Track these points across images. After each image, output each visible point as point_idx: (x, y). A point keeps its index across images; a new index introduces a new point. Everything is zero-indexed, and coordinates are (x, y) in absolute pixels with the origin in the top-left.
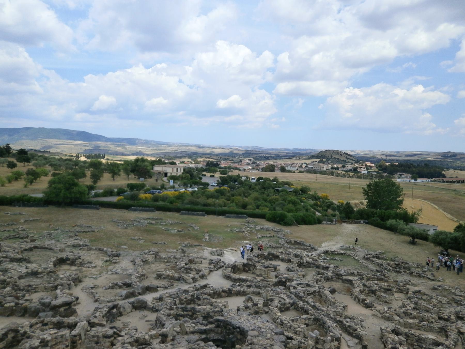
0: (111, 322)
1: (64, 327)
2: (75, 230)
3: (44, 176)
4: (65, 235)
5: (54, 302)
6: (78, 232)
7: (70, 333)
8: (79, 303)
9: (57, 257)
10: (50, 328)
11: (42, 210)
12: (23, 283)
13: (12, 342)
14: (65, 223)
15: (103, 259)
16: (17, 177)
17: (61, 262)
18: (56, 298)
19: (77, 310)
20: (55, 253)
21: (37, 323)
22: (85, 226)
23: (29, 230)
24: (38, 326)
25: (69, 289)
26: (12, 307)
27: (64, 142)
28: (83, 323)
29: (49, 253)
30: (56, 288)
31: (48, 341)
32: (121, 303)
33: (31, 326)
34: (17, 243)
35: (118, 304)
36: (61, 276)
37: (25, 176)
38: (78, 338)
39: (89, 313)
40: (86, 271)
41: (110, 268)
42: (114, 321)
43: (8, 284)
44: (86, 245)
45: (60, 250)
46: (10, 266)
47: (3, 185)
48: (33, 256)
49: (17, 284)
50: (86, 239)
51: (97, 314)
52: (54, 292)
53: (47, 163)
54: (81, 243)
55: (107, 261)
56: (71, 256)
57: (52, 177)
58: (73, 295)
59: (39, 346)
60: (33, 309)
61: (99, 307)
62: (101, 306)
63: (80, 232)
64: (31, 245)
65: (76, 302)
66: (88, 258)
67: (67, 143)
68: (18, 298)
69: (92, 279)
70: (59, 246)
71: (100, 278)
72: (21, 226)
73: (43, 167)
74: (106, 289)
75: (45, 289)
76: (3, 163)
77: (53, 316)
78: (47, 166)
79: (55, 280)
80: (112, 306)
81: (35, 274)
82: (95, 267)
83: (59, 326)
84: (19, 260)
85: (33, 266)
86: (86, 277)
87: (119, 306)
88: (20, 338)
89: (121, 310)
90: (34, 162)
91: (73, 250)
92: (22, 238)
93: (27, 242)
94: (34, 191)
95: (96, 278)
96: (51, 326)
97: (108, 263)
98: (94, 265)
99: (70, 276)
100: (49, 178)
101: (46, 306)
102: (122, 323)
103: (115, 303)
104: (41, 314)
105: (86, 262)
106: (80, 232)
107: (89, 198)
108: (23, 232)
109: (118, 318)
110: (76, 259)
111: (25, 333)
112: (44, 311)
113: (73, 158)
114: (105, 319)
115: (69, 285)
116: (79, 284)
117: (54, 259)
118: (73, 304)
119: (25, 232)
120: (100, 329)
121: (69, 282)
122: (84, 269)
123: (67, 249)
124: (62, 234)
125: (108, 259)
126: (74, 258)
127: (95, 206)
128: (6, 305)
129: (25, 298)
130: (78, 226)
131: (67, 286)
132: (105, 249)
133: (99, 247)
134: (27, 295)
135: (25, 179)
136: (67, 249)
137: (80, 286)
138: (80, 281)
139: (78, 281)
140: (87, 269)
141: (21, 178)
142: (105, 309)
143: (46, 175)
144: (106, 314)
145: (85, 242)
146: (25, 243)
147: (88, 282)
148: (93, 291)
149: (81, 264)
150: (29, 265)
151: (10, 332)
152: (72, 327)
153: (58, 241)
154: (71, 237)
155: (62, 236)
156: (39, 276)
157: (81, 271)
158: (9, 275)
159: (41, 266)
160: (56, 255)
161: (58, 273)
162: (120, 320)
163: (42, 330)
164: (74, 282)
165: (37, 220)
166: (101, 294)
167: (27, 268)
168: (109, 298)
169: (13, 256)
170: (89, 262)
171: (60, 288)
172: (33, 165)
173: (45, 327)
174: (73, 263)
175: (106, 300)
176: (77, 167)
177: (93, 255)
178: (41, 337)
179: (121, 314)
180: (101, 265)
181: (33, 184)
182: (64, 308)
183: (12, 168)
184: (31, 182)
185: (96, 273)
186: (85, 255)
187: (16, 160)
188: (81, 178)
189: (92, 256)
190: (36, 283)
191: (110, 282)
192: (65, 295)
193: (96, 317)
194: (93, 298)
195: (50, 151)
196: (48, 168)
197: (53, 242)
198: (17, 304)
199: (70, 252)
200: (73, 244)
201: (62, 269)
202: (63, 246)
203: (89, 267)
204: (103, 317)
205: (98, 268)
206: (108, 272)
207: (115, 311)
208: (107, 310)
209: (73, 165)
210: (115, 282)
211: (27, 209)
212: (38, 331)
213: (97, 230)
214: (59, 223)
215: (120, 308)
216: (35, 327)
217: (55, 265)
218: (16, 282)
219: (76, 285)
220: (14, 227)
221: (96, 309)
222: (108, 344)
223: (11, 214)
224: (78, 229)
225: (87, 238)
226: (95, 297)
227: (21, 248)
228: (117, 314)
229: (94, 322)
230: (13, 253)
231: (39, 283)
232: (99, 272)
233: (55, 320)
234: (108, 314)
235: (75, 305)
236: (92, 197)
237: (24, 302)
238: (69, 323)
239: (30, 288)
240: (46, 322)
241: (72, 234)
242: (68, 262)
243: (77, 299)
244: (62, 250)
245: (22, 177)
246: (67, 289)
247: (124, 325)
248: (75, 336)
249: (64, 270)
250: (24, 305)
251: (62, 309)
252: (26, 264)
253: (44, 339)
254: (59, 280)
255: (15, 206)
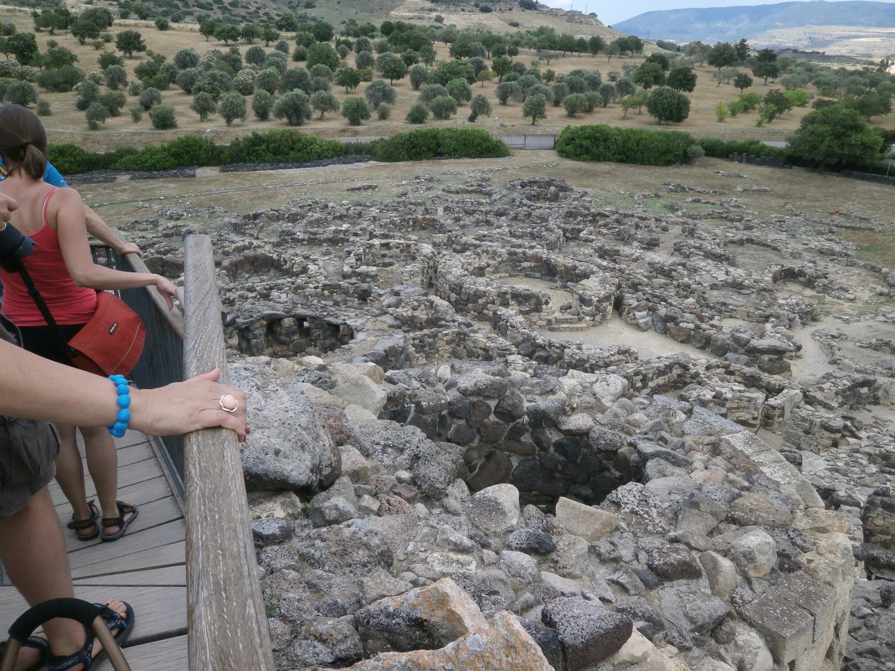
0: (851, 408)
1: (759, 388)
2: (832, 221)
3: (798, 106)
4: (809, 228)
5: (756, 343)
6: (837, 226)
7: (766, 400)
8: (799, 357)
9: (783, 266)
10: (736, 381)
11: (779, 172)
12: (715, 296)
13: (675, 382)
14: (817, 204)
15: (875, 288)
16: (747, 105)
17: (789, 275)
18: (762, 336)
19: (792, 368)
20: (782, 257)
21: (718, 367)
22: (856, 217)
23: (747, 208)
24: (718, 371)
25: (790, 327)
26: (690, 329)
27: (861, 31)
28: (793, 392)
29: (771, 255)
30: (767, 319)
31: (726, 399)
32: (882, 380)
33: (708, 368)
34: (722, 227)
35: (875, 381)
36: (781, 301)
37: (762, 105)
38: (777, 412)
39: (811, 378)
40: (833, 304)
41: (884, 309)
42: (858, 409)
43: (692, 292)
44: (846, 255)
45: (792, 254)
46: (702, 264)
47: (721, 120)
48: (743, 255)
49: (705, 296)
50: (851, 243)
51: (826, 386)
52: (761, 325)
53: (811, 79)
54: (837, 248)
55: (881, 294)
56: (809, 269)
57: (813, 109)
58: (793, 340)
59: (711, 401)
60: (719, 343)
61: (834, 374)
62: (838, 374)
63: (842, 227)
64: (744, 234)
65: (794, 354)
66: (844, 280)
67: (866, 34)
68: (701, 319)
69: (838, 320)
70: (793, 245)
71: (857, 323)
72: (735, 199)
73: (801, 87)
74: (861, 347)
75: (748, 316)
76: (729, 77)
77: (747, 364)
78: (809, 84)
79: (769, 306)
80: (860, 381)
81: (737, 286)
82: (851, 300)
83: (751, 382)
84: (718, 258)
85: (738, 273)
86: (827, 314)
87: (876, 385)
88: (688, 380)
89: (880, 393)
90: (785, 76)
91: (818, 259)
92: (732, 220)
93: (737, 229)
94: (773, 135)
95: (847, 322)
96: (739, 379)
97: (883, 299)
98: (852, 297)
99: (797, 304)
100: (808, 111)
101: (741, 345)
102: (874, 417)
103: (872, 378)
104: (729, 355)
105: (836, 287)
106: (842, 227)
107: (883, 158)
108: (735, 209)
109: (868, 407)
110: (818, 277)
111: (697, 375)
112: (736, 351)
113: (873, 67)
114: (840, 399)
115: (791, 320)
116: (810, 323)
117: (776, 269)
118: (788, 354)
119: (738, 210)
120: (823, 413)
121: (792, 316)
122: (828, 298)
123: (805, 254)
124: (805, 226)
125: (886, 290)
126: (815, 275)
127: (891, 178)
128: (681, 324)
129: (712, 322)
130: (840, 214)
131: (787, 321)
132: (884, 270)
133: (874, 264)
134: (716, 317)
135: (761, 110)
136: (805, 254)
137: (810, 329)
138: (815, 319)
139: (809, 317)
140: (835, 300)
141: (754, 109)
142: (845, 382)
143: (803, 104)
144: (844, 391)
145: (845, 248)
146: (734, 231)
147: (828, 325)
148: (835, 344)
149: (826, 289)
150: (731, 269)
151: (677, 366)
152: (772, 391)
153: (794, 236)
154: (820, 233)
155: (803, 229)
156: (743, 291)
157: (821, 302)
158: (697, 278)
159: (751, 275)
160: (783, 262)
161: (778, 295)
162: (869, 411)
163: (722, 380)
164: (801, 318)
165: (766, 191)
166: (847, 352)
167: (727, 273)
168: (862, 365)
169: (709, 248)
170: (841, 288)
171: (772, 322)
172: (782, 83)
173: (728, 377)
174: (810, 283)
175: (854, 366)
176: (873, 89)
177: (854, 277)
178: (717, 389)
179: (876, 401)
180: (866, 298)
181: (774, 121)
182: (770, 356)
183: (742, 88)
184: (771, 117)
185: (851, 312)
186: (837, 273)
187: (753, 71)
188: (876, 113)
189: (851, 278)
190: (735, 303)
191: (874, 336)
192: (779, 335)
193: (821, 389)
194: (830, 356)
195: (824, 53)
196: (811, 89)
197: (784, 236)
198: (697, 327)
199: (810, 262)
200: (819, 246)
201: (786, 288)
202: (800, 247)
203: (839, 298)
204: (837, 394)
205: (859, 304)
206: (877, 315)
207: (865, 390)
208: (849, 384)
209: (865, 85)
210: (886, 339)
211: (753, 168)
212: (716, 379)
213: (880, 229)
214: (805, 203)
215: (878, 389)
216: (713, 371)
217: (775, 279)
218: (704, 293)
219: (804, 324)
220: (724, 199)
221: (828, 377)
222: (828, 442)
223: (723, 175)
224: (838, 220)
225: (852, 240)
226: (833, 354)
227: (726, 236)
228: (868, 397)
229: (814, 397)
230: (710, 244)
231: (740, 304)
232: (856, 312)
233: (747, 370)
234: (848, 393)
235: (791, 358)
236: (890, 158)
237: (708, 327)
238: (769, 383)
239: (723, 308)
240: (732, 368)
241: (823, 228)
242: (802, 279)
243: (799, 348)
244: (794, 255)
245: (757, 106)
246: (784, 326)
247: (876, 422)
248: (773, 408)
249: (791, 291)
250: (707, 332)
251: (766, 358)
252: (727, 266)
253: (722, 394)
254: (776, 307)
255: (732, 160)
